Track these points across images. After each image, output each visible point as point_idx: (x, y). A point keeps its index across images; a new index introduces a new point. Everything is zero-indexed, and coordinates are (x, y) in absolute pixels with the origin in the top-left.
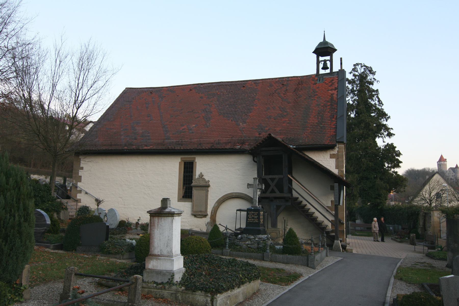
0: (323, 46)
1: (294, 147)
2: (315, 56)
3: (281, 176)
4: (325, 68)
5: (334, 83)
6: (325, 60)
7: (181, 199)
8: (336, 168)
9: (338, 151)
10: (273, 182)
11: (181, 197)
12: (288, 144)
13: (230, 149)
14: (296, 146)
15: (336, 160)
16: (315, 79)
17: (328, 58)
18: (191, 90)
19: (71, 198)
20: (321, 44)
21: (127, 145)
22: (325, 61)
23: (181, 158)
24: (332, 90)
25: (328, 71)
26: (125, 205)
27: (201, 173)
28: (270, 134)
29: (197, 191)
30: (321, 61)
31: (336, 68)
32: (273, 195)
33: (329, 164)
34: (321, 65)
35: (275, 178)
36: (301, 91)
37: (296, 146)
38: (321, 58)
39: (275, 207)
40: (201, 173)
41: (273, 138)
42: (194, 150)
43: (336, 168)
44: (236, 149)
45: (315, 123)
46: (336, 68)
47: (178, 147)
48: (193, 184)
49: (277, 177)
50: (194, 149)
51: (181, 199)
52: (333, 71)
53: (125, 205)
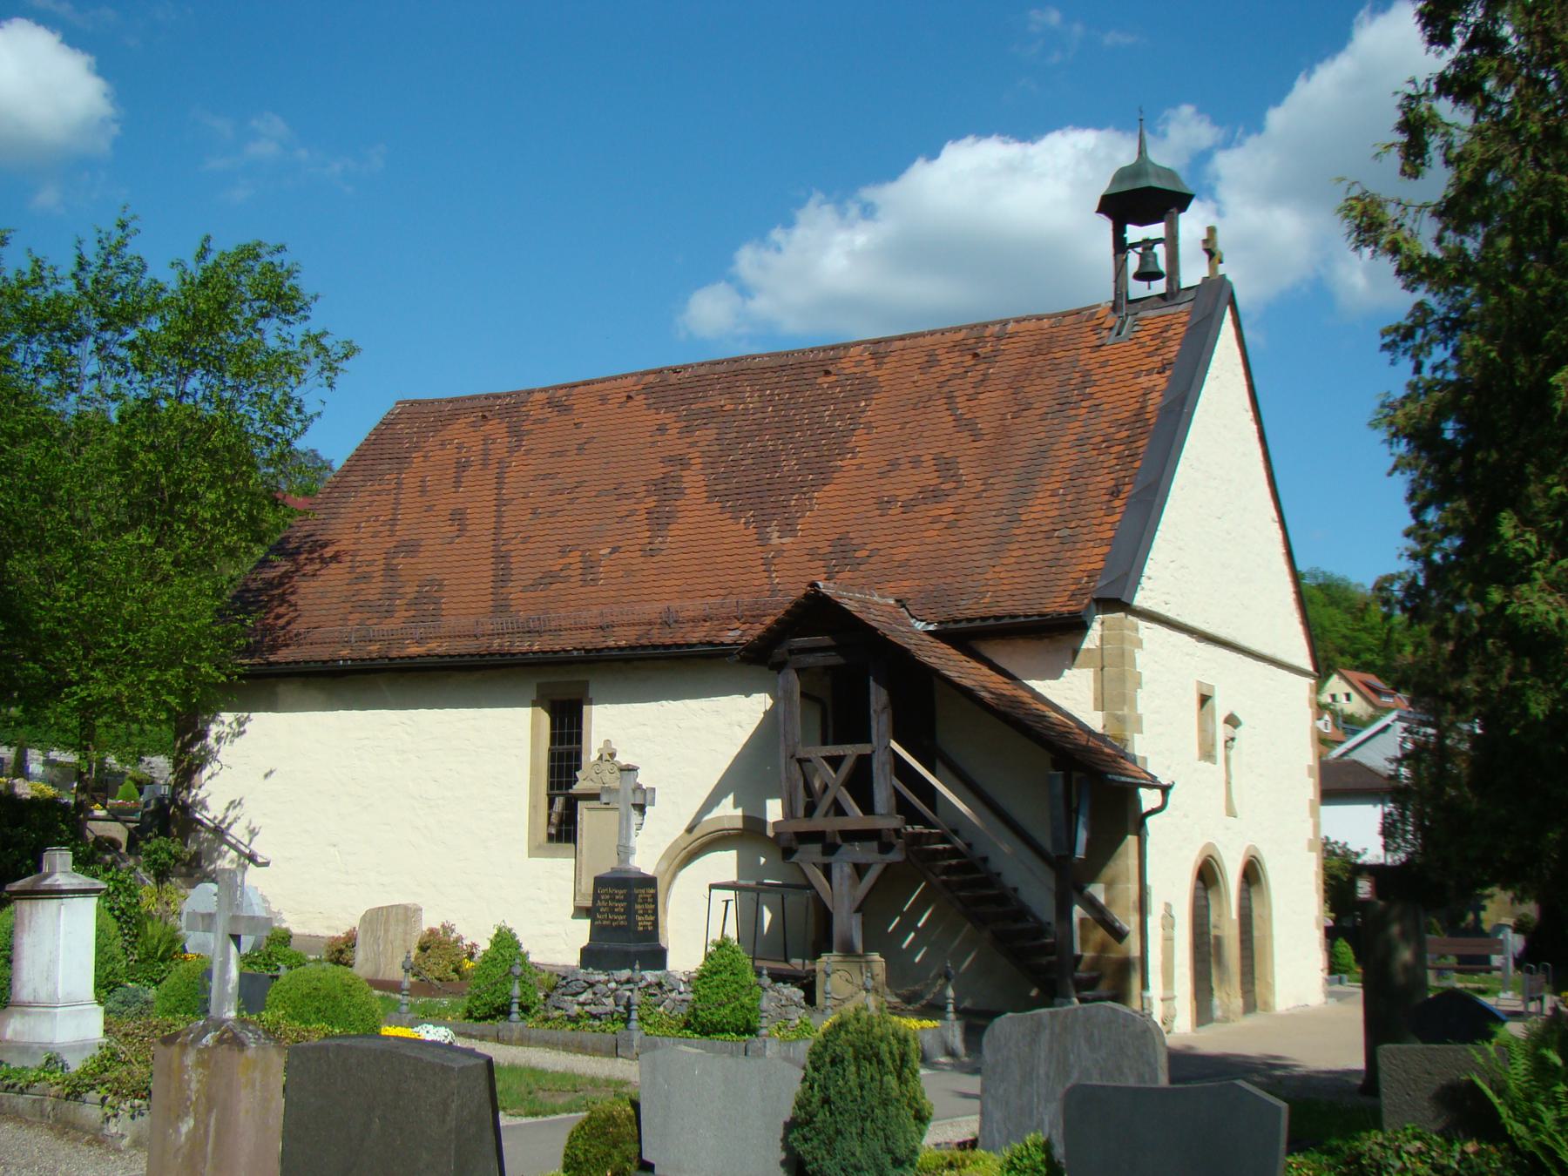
0: (1126, 187)
1: (931, 628)
2: (1106, 225)
3: (864, 749)
4: (1146, 275)
5: (1170, 339)
6: (1146, 241)
7: (539, 847)
8: (1096, 709)
9: (1102, 638)
10: (836, 771)
11: (543, 836)
12: (913, 617)
13: (701, 643)
14: (940, 623)
15: (1096, 674)
16: (1104, 326)
17: (1157, 230)
18: (629, 397)
19: (1322, 835)
20: (1121, 175)
21: (353, 639)
22: (1148, 244)
23: (539, 686)
24: (1149, 372)
25: (1160, 286)
26: (347, 873)
27: (608, 742)
28: (813, 585)
29: (593, 812)
30: (1134, 246)
31: (1193, 272)
32: (839, 824)
33: (1071, 689)
34: (1133, 261)
35: (845, 756)
36: (1038, 381)
37: (940, 623)
38: (1134, 233)
39: (848, 869)
40: (608, 742)
41: (826, 598)
42: (575, 653)
43: (1096, 709)
44: (722, 644)
45: (1043, 522)
46: (1193, 272)
47: (523, 645)
48: (578, 788)
49: (851, 751)
50: (575, 649)
51: (539, 847)
52: (1183, 285)
53: (347, 873)
